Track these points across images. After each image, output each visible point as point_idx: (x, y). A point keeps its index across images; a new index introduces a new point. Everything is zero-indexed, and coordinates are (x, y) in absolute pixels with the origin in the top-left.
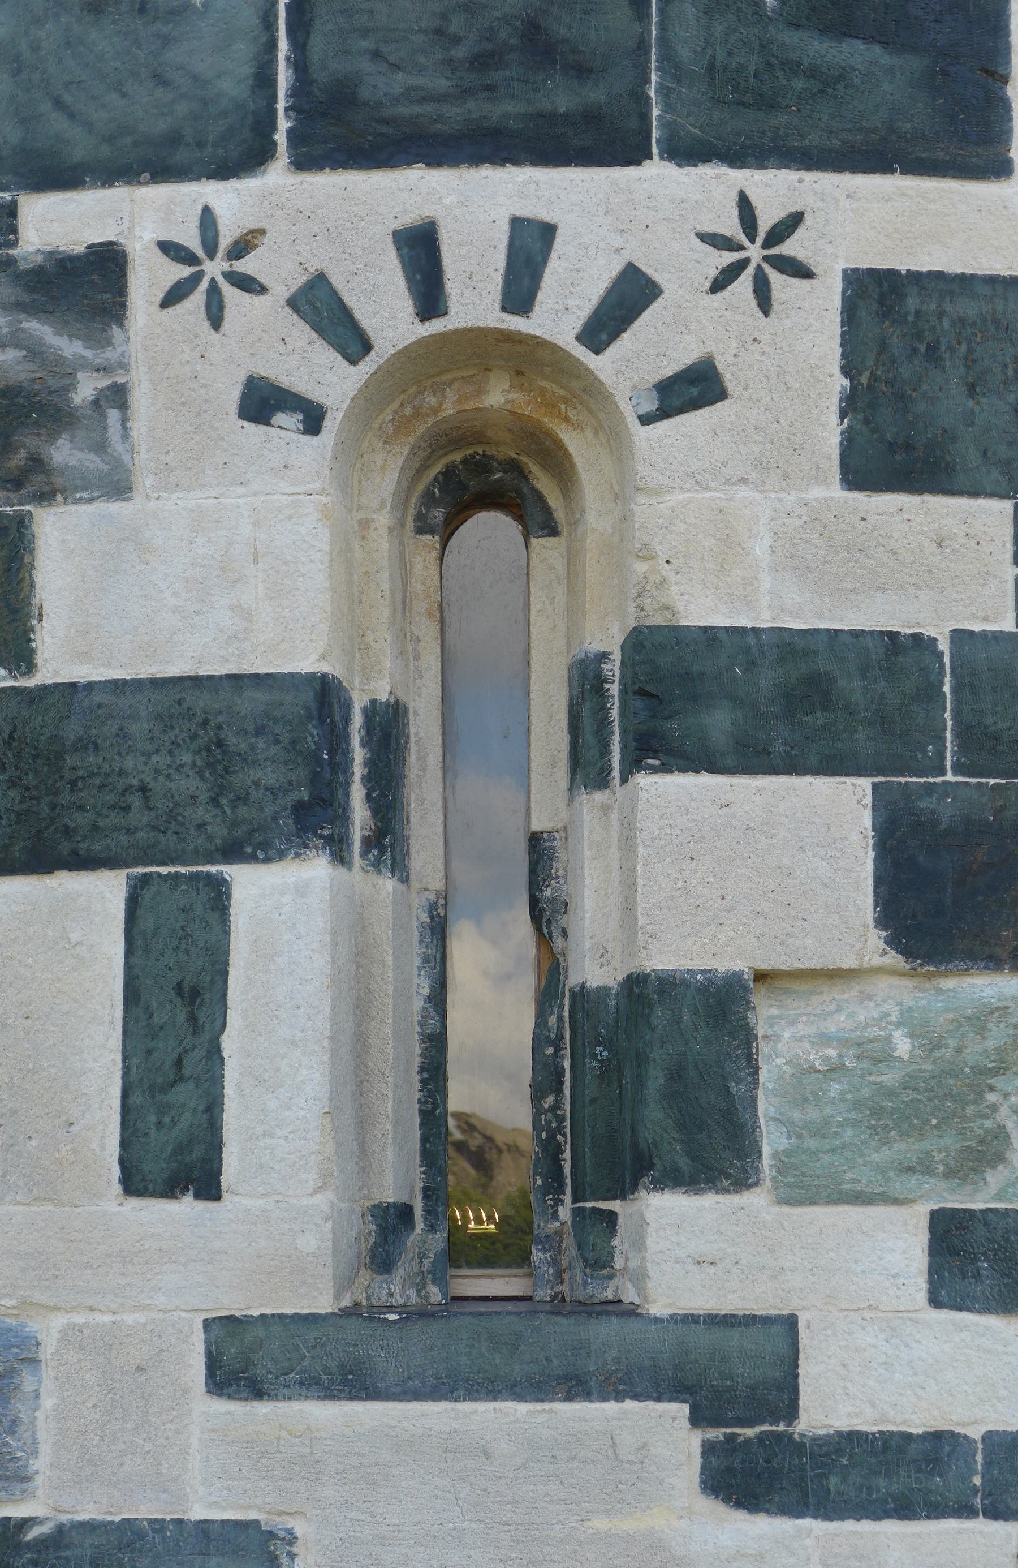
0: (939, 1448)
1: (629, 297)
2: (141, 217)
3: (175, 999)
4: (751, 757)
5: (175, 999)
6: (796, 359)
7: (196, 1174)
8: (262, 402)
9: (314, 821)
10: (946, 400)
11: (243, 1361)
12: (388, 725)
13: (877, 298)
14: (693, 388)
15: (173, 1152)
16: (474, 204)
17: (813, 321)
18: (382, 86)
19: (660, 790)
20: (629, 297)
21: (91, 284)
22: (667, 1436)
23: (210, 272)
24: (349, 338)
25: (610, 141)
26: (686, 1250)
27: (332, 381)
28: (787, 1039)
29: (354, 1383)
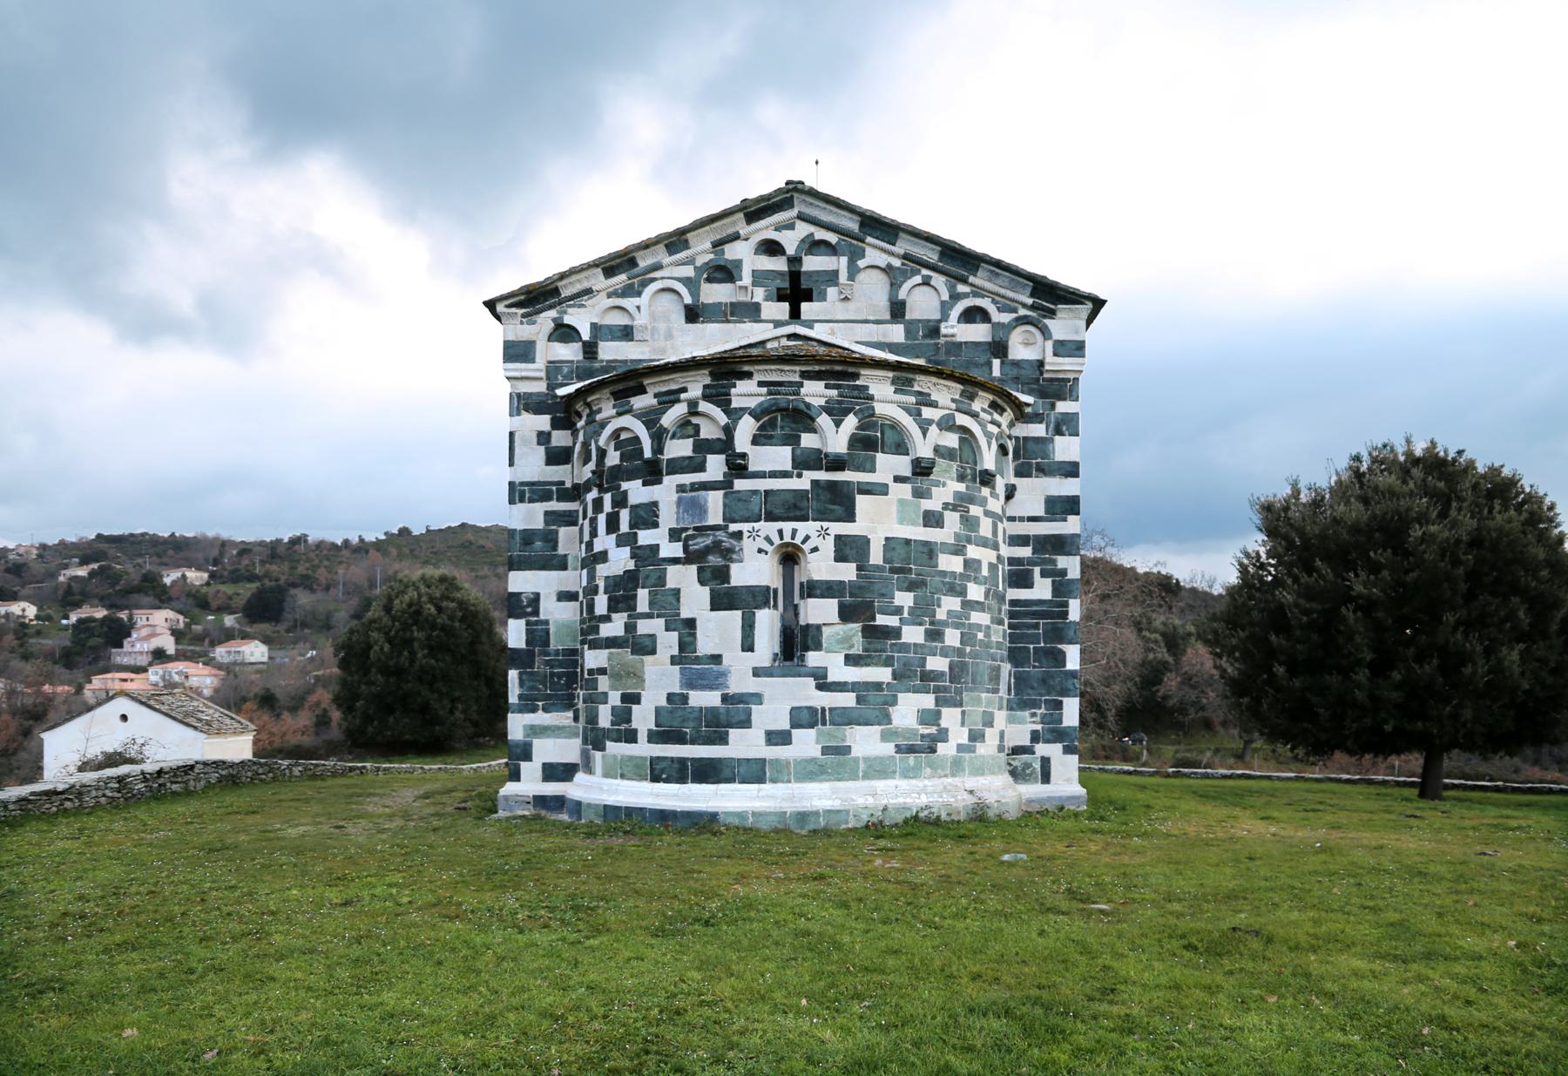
0: (845, 683)
1: (807, 538)
2: (745, 527)
3: (748, 627)
4: (822, 596)
5: (748, 627)
6: (828, 546)
7: (751, 649)
8: (760, 551)
9: (766, 604)
10: (848, 551)
11: (757, 672)
12: (775, 591)
13: (838, 538)
14: (815, 549)
15: (748, 646)
16: (787, 527)
17: (830, 541)
18: (776, 511)
19: (810, 601)
20: (807, 538)
21: (738, 535)
22: (811, 682)
23: (754, 534)
24: (771, 543)
25: (805, 519)
26: (813, 659)
27: (769, 548)
28: (826, 631)
29: (771, 675)
